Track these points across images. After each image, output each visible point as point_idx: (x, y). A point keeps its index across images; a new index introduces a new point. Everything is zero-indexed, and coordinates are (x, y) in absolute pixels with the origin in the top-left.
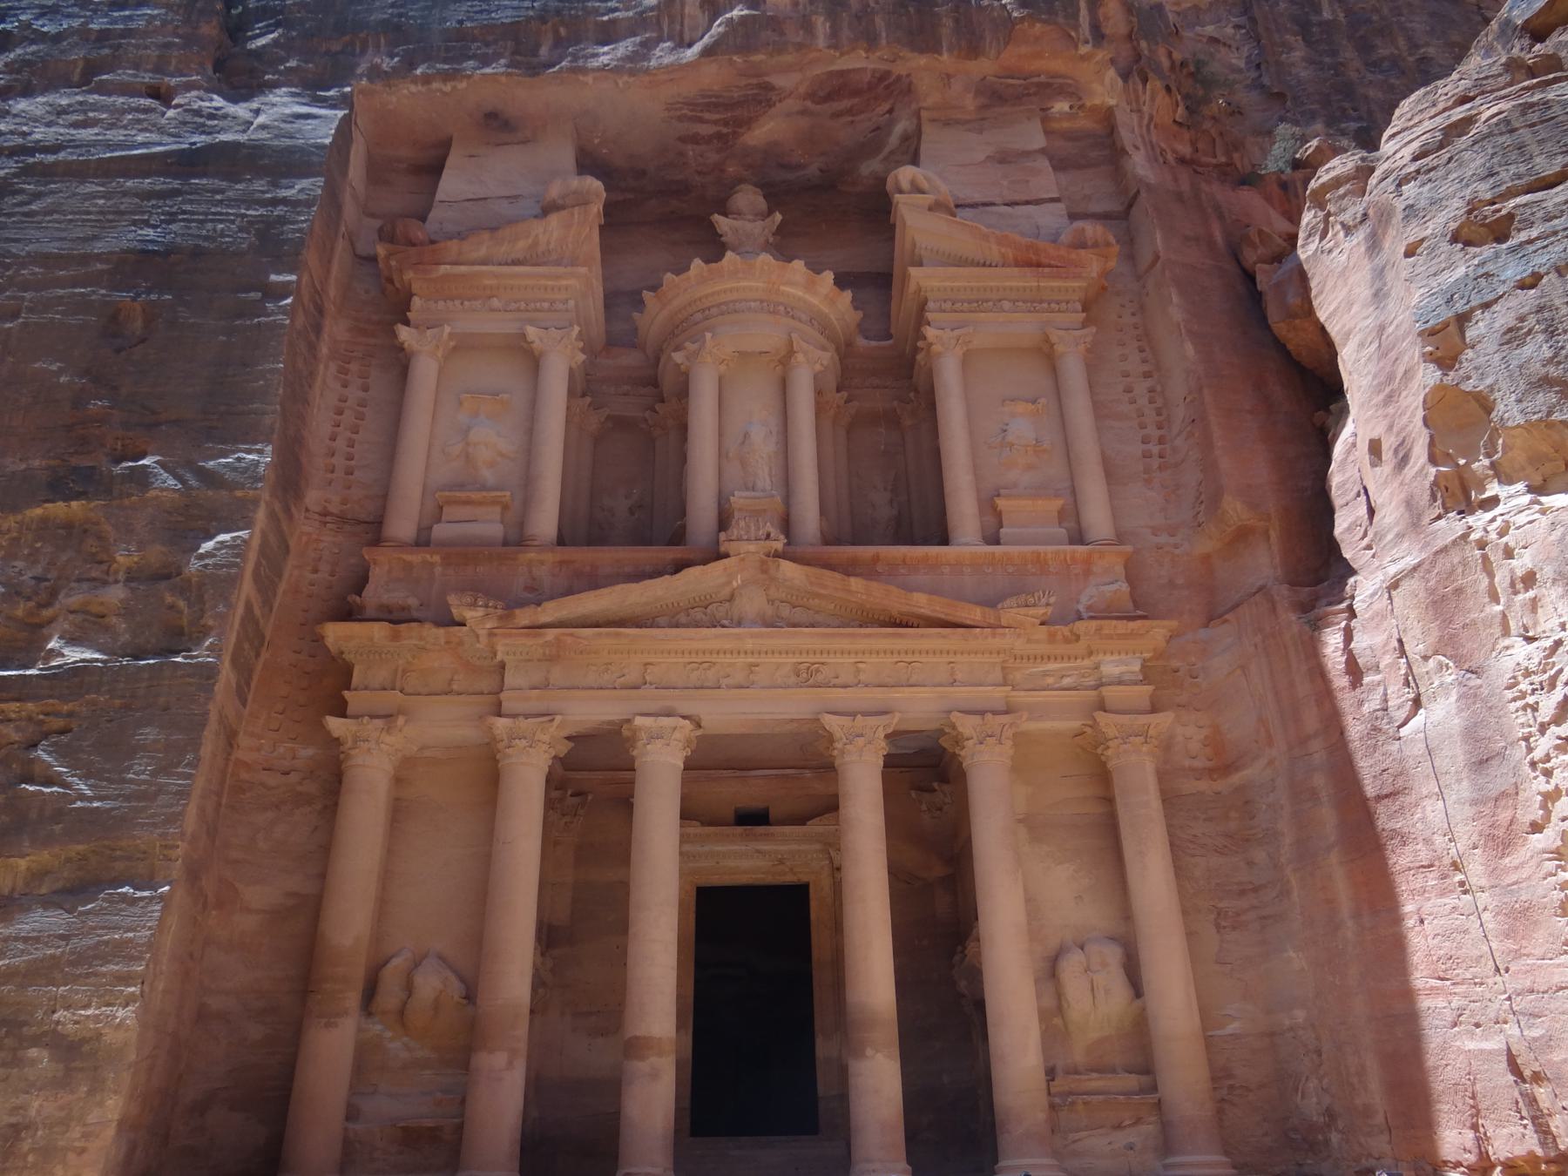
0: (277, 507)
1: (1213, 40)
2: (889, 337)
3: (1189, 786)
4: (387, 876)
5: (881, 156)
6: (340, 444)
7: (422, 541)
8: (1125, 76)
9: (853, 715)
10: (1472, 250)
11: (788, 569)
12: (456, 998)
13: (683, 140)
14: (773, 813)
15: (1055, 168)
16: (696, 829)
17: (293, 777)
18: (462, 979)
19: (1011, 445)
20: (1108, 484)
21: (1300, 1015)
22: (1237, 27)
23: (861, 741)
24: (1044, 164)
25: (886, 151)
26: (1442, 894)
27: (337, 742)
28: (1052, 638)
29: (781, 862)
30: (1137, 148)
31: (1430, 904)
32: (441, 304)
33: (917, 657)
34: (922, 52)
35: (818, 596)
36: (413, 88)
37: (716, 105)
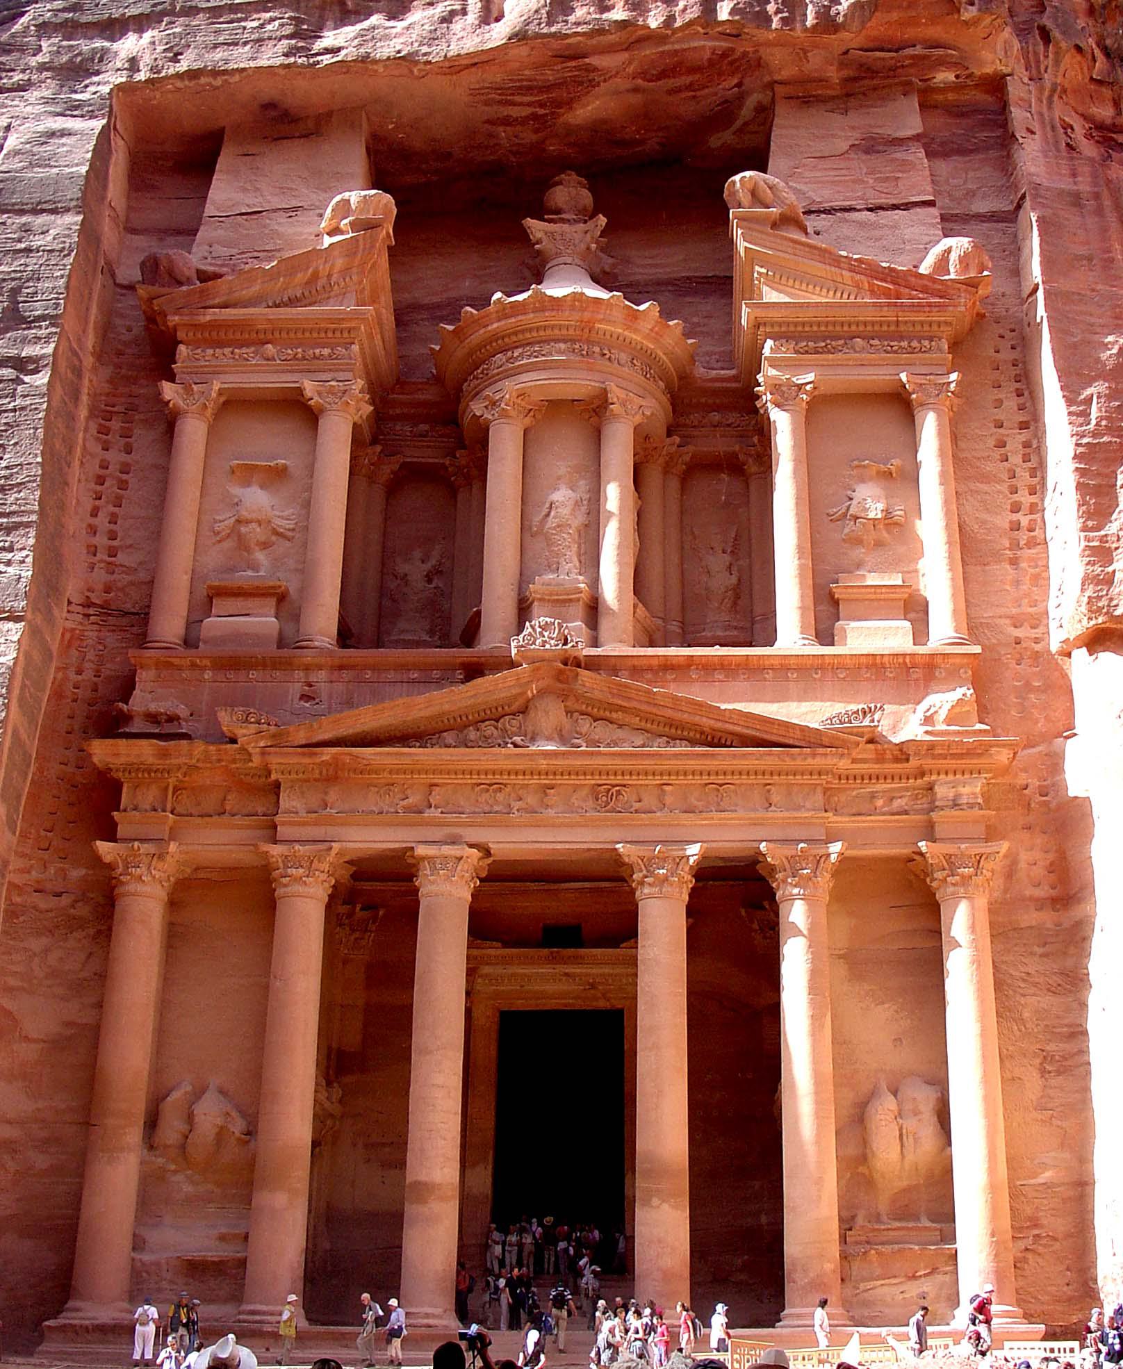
0: (39, 619)
4: (164, 1005)
5: (733, 129)
6: (102, 521)
7: (189, 642)
12: (237, 1134)
13: (488, 122)
16: (494, 951)
17: (65, 900)
18: (243, 1114)
24: (917, 154)
25: (738, 123)
27: (110, 867)
29: (593, 986)
30: (1033, 133)
32: (210, 351)
33: (729, 778)
36: (179, 84)
37: (530, 88)
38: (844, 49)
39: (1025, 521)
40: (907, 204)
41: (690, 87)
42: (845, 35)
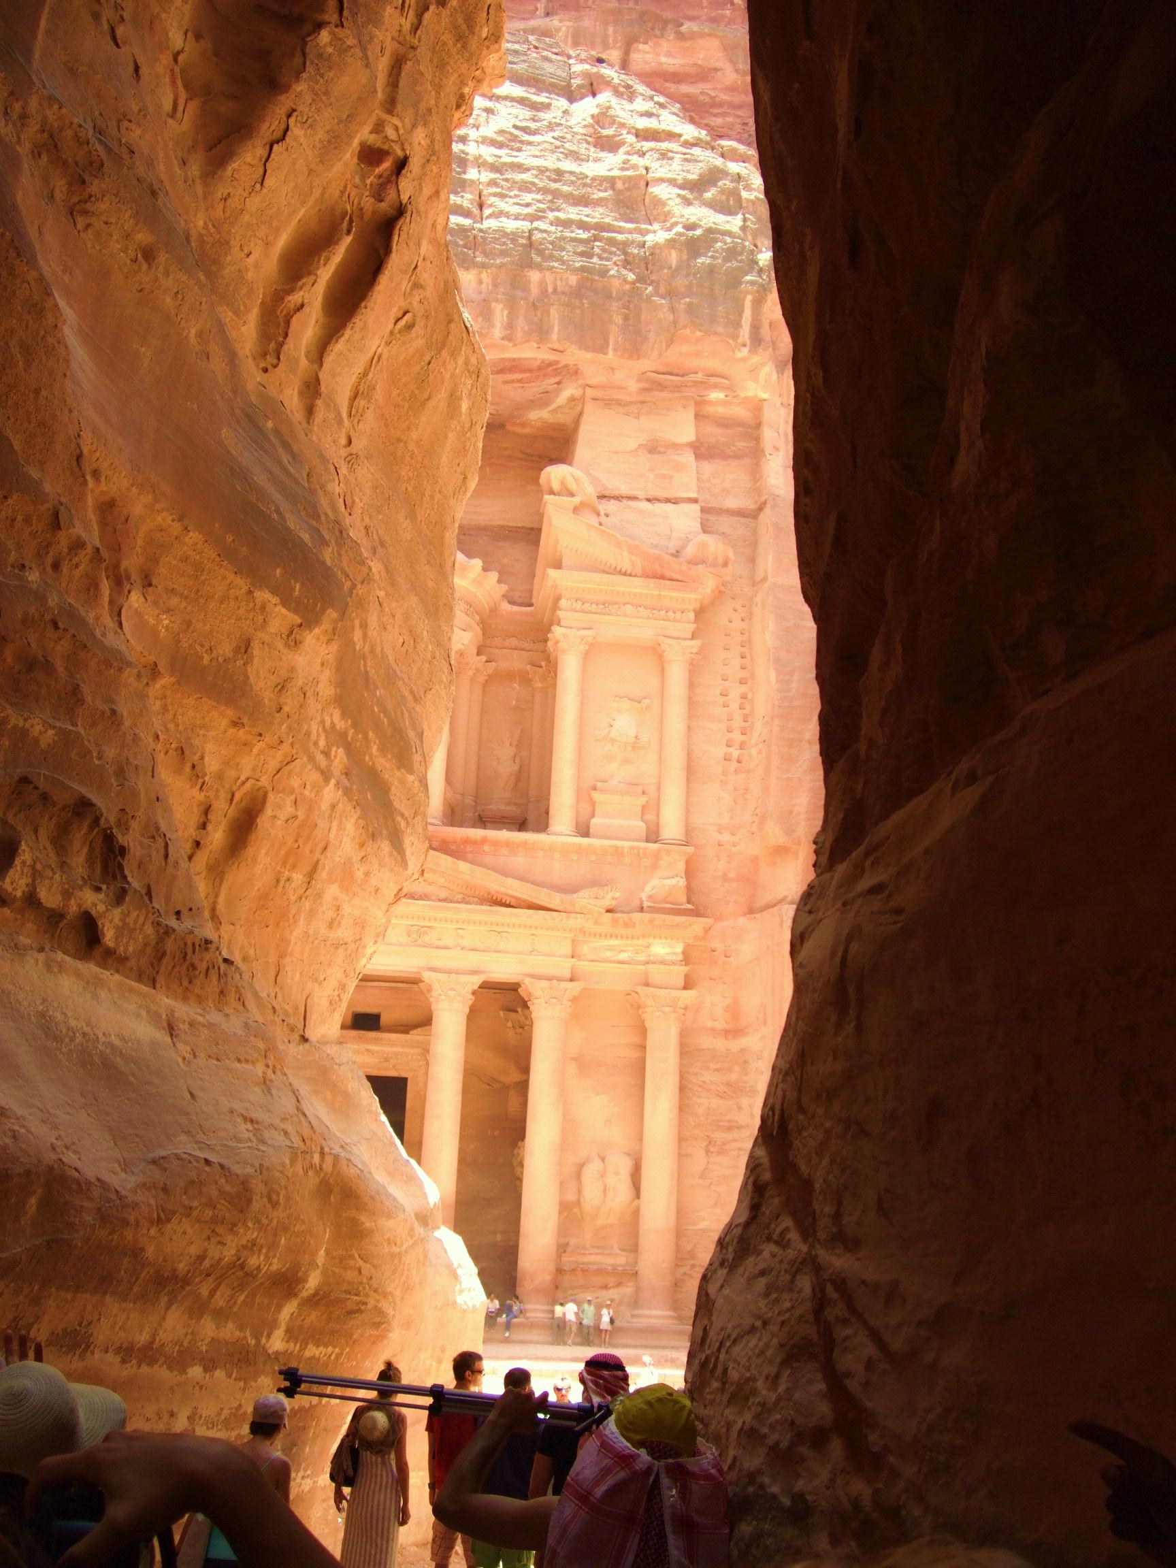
2: (531, 605)
3: (707, 1042)
5: (550, 408)
9: (449, 972)
15: (699, 456)
19: (613, 741)
20: (688, 781)
24: (689, 458)
30: (776, 449)
34: (587, 349)
39: (735, 753)
41: (520, 381)
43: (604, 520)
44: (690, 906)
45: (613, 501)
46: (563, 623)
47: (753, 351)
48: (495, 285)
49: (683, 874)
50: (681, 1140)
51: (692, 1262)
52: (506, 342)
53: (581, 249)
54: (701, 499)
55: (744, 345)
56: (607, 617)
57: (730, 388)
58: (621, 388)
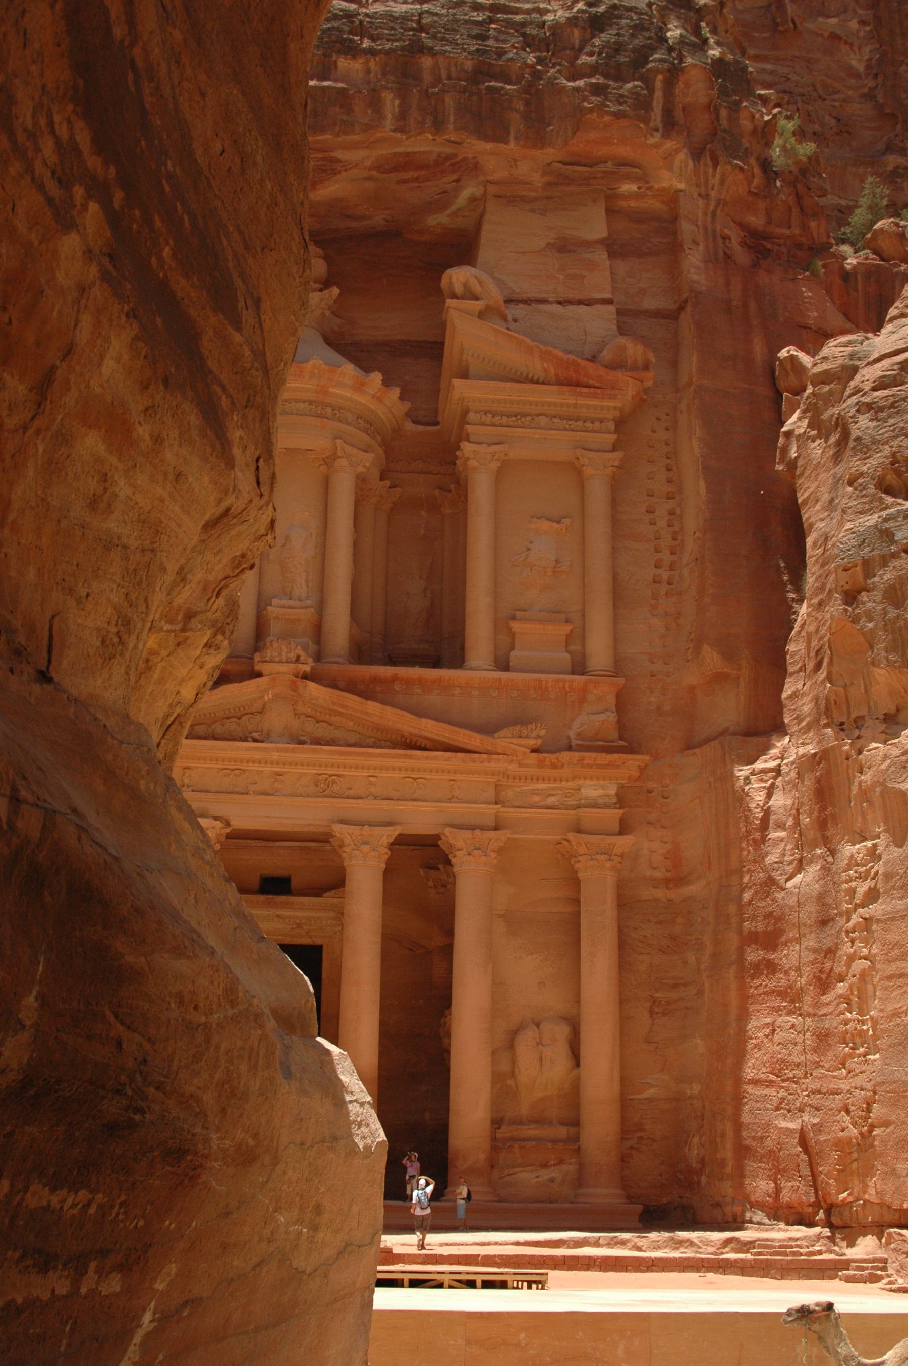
1: (834, 37)
2: (437, 424)
3: (647, 893)
5: (449, 212)
8: (697, 154)
10: (889, 499)
11: (313, 689)
14: (294, 883)
15: (612, 255)
20: (615, 606)
21: (696, 1088)
22: (863, 23)
23: (365, 848)
24: (601, 256)
25: (454, 208)
26: (788, 1014)
28: (541, 764)
29: (299, 926)
30: (695, 242)
31: (780, 1020)
35: (341, 714)
38: (548, 162)
39: (665, 575)
40: (589, 300)
41: (416, 180)
42: (550, 151)
43: (512, 325)
44: (622, 743)
45: (521, 305)
46: (472, 438)
47: (666, 135)
48: (384, 74)
49: (614, 709)
50: (622, 1001)
51: (639, 1134)
52: (399, 135)
53: (475, 31)
54: (615, 301)
55: (657, 130)
56: (520, 430)
57: (643, 178)
58: (528, 183)
